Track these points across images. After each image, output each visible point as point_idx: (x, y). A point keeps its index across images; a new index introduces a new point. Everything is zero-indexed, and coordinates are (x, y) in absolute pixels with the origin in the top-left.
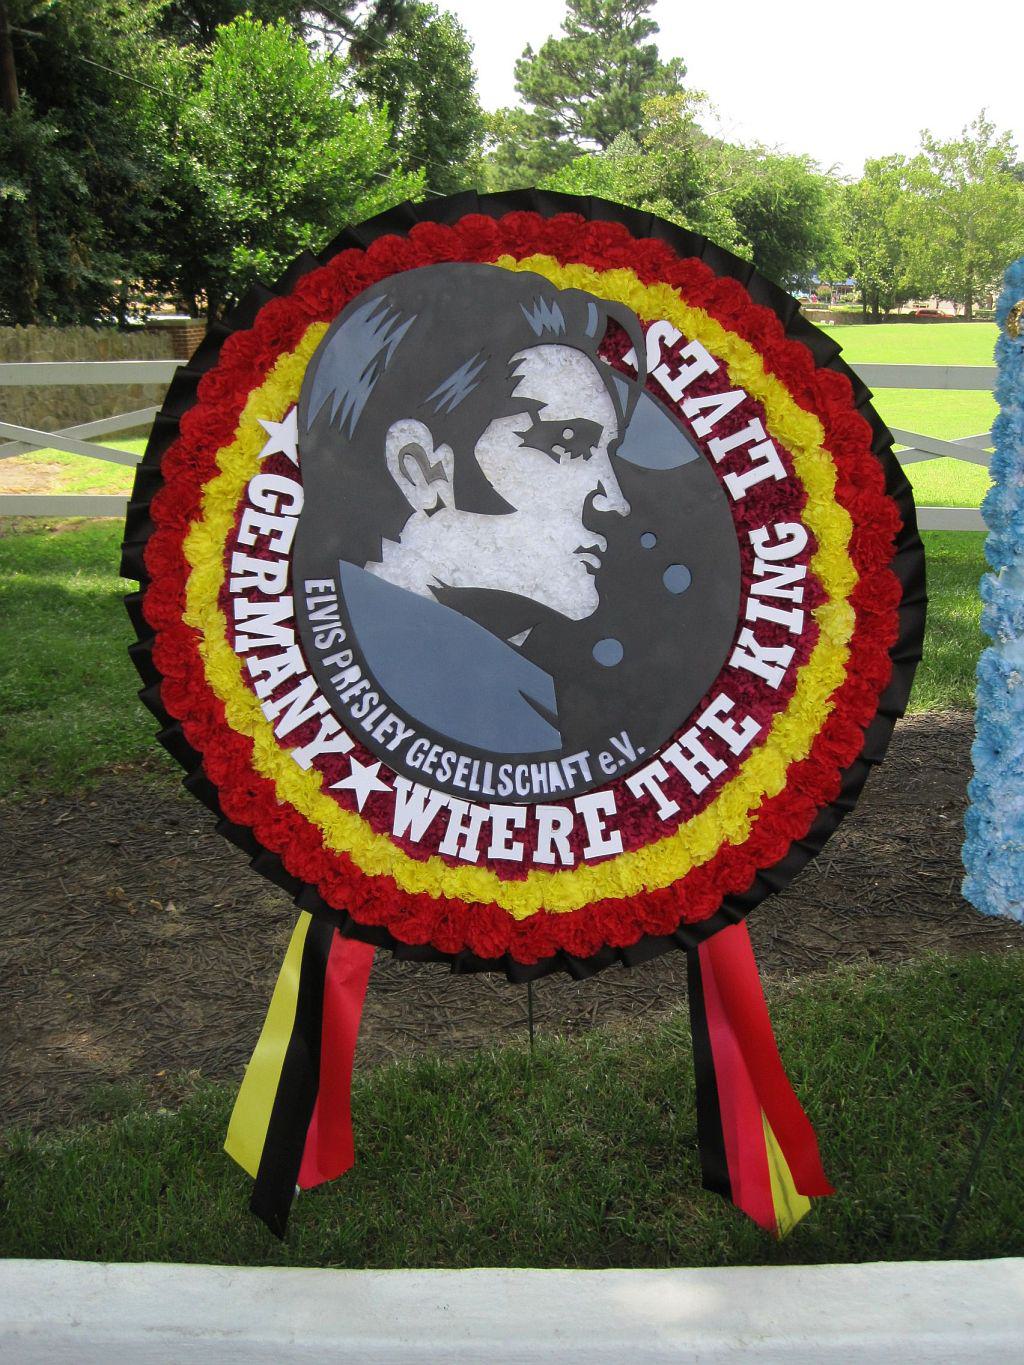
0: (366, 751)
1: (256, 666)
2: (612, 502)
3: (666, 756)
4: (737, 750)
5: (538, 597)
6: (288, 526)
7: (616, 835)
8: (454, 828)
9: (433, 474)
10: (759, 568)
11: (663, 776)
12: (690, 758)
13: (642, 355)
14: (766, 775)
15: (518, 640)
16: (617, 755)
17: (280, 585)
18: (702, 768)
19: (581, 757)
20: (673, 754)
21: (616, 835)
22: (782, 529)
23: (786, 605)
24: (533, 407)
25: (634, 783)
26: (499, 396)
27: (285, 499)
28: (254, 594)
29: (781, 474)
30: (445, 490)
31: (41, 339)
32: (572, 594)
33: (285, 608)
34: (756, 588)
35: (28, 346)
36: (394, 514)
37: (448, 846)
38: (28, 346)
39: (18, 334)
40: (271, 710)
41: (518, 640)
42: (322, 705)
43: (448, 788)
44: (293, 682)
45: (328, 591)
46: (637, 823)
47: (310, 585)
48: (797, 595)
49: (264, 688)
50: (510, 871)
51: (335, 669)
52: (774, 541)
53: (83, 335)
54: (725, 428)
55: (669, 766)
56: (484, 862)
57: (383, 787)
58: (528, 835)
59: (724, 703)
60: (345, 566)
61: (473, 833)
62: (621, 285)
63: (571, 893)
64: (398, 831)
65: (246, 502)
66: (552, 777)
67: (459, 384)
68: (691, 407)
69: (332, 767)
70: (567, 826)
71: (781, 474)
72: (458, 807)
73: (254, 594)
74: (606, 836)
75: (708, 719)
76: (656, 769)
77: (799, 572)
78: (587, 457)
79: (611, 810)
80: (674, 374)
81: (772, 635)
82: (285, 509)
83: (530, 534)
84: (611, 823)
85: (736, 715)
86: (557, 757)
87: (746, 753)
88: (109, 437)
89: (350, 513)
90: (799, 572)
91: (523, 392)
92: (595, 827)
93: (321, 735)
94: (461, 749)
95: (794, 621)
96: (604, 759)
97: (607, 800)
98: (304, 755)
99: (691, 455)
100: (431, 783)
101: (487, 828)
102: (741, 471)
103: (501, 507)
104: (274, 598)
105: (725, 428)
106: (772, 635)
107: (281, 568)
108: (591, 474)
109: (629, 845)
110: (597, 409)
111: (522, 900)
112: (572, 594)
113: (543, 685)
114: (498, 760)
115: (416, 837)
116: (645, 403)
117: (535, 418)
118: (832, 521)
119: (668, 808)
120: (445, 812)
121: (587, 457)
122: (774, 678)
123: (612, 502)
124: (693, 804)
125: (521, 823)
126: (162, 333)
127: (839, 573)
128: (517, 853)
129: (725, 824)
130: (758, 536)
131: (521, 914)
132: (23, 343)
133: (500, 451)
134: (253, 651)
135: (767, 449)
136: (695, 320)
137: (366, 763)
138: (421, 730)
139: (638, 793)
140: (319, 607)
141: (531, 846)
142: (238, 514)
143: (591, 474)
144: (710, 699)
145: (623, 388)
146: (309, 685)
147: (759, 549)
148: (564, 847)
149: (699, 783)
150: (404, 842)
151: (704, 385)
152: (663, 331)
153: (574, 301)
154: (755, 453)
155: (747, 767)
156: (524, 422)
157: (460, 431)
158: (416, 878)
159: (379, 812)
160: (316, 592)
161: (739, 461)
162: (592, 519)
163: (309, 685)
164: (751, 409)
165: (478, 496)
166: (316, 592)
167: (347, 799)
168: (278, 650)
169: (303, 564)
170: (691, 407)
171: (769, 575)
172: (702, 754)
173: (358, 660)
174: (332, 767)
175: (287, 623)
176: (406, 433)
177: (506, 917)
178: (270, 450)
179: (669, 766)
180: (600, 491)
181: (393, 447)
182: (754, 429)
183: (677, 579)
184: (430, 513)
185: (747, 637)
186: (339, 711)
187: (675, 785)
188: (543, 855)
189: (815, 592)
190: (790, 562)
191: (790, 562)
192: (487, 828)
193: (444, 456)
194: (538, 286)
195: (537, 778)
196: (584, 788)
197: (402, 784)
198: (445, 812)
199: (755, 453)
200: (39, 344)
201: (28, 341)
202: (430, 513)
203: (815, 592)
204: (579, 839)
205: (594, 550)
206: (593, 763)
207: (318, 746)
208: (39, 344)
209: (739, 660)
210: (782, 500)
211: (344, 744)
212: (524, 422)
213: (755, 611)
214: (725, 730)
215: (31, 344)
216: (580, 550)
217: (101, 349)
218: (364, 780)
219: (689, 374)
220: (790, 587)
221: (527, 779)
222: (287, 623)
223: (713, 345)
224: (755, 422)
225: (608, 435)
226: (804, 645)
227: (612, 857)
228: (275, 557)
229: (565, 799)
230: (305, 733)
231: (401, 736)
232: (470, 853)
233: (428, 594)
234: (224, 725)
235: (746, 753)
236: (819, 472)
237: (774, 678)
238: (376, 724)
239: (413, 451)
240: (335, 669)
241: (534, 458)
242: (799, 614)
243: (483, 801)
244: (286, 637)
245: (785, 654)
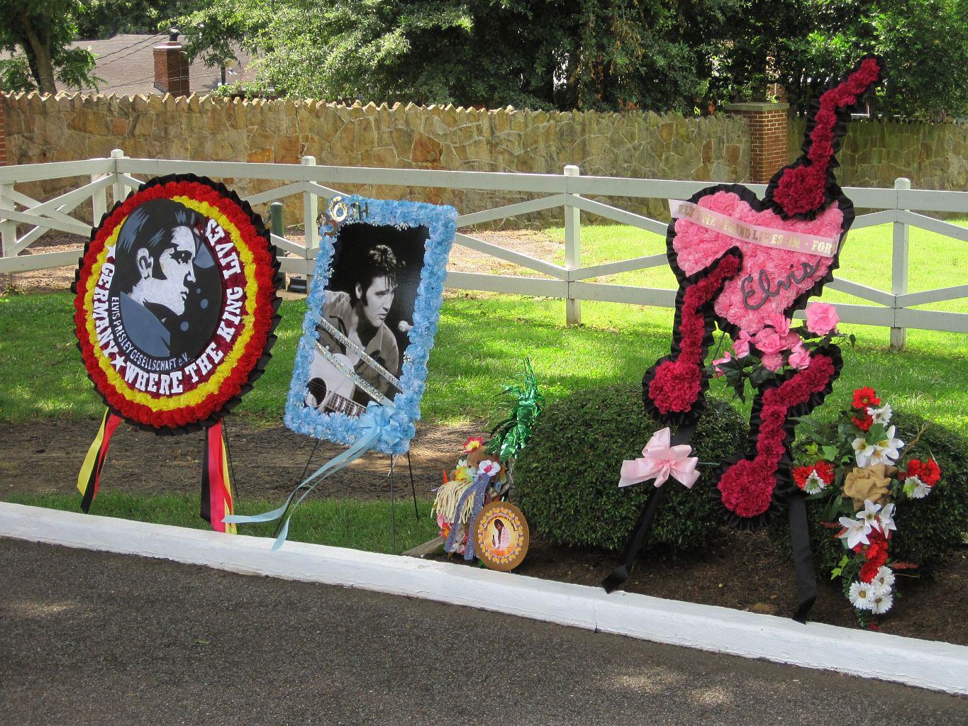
0: (121, 353)
1: (98, 323)
2: (192, 278)
3: (197, 362)
4: (216, 362)
5: (171, 307)
6: (110, 279)
7: (181, 386)
8: (139, 379)
9: (148, 266)
10: (228, 302)
11: (195, 368)
12: (203, 363)
13: (205, 231)
14: (224, 371)
15: (163, 320)
16: (183, 360)
17: (106, 298)
18: (206, 367)
19: (174, 360)
20: (199, 361)
21: (181, 386)
22: (236, 289)
23: (235, 315)
24: (175, 246)
25: (187, 370)
26: (167, 242)
27: (111, 271)
28: (99, 300)
29: (239, 271)
30: (150, 270)
31: (598, 123)
32: (179, 308)
33: (106, 306)
34: (227, 308)
35: (583, 130)
36: (137, 277)
37: (137, 385)
38: (583, 130)
39: (573, 119)
40: (99, 337)
41: (163, 320)
42: (112, 336)
43: (139, 366)
44: (105, 329)
45: (117, 301)
46: (187, 384)
47: (113, 298)
48: (238, 311)
49: (98, 330)
50: (156, 395)
51: (116, 326)
52: (233, 293)
53: (645, 120)
54: (226, 255)
55: (197, 365)
56: (146, 391)
57: (124, 365)
58: (158, 384)
59: (213, 345)
60: (122, 293)
61: (144, 381)
62: (203, 208)
63: (171, 405)
64: (126, 380)
65: (101, 272)
66: (165, 365)
67: (157, 237)
68: (218, 248)
69: (112, 356)
70: (168, 382)
71: (239, 271)
72: (141, 372)
73: (99, 300)
74: (178, 387)
75: (208, 350)
76: (193, 366)
77: (240, 304)
78: (187, 263)
79: (180, 378)
80: (213, 237)
81: (229, 324)
82: (111, 275)
83: (167, 288)
84: (180, 382)
85: (216, 350)
86: (167, 359)
87: (222, 361)
88: (483, 227)
89: (126, 278)
90: (240, 304)
91: (173, 241)
92: (175, 383)
93: (110, 347)
94: (145, 354)
95: (236, 320)
96: (180, 361)
97: (179, 374)
98: (106, 352)
99: (211, 263)
100: (135, 364)
101: (148, 380)
102: (228, 270)
103: (163, 277)
104: (104, 302)
105: (226, 255)
106: (229, 324)
107: (107, 293)
108: (189, 268)
109: (185, 391)
110: (193, 250)
111: (155, 405)
112: (179, 308)
113: (167, 335)
114: (154, 358)
115: (130, 382)
116: (203, 245)
117: (175, 249)
118: (252, 287)
119: (195, 379)
120: (138, 374)
121: (187, 263)
122: (228, 339)
123: (192, 278)
124: (204, 379)
125: (156, 380)
126: (737, 117)
127: (251, 305)
128: (154, 389)
129: (212, 386)
130: (229, 291)
131: (154, 410)
132: (578, 128)
133: (166, 259)
134: (97, 319)
135: (236, 263)
136: (223, 219)
137: (121, 356)
138: (136, 348)
139: (188, 373)
140: (115, 306)
141: (158, 389)
142: (100, 275)
143: (189, 268)
144: (207, 345)
145: (198, 241)
146: (110, 330)
147: (229, 296)
148: (167, 388)
149: (204, 372)
150: (127, 383)
151: (220, 241)
152: (212, 223)
153: (189, 212)
154: (232, 264)
155: (218, 368)
156: (172, 251)
157: (156, 253)
158: (128, 395)
159: (123, 371)
160: (114, 301)
161: (229, 266)
162: (186, 283)
163: (110, 330)
164: (234, 249)
165: (158, 274)
166: (114, 301)
167: (114, 366)
168: (102, 319)
169: (113, 292)
170: (218, 248)
171: (232, 304)
172: (207, 362)
173: (122, 324)
174: (112, 356)
175: (106, 310)
176: (143, 252)
177: (149, 409)
178: (109, 256)
179: (197, 365)
180: (189, 274)
181: (139, 257)
182: (234, 255)
183: (204, 304)
184: (145, 278)
185: (222, 324)
186: (115, 339)
187: (198, 371)
188: (161, 391)
189: (244, 312)
190: (237, 300)
191: (237, 300)
192: (148, 380)
193: (151, 260)
194: (181, 206)
195: (162, 365)
196: (173, 370)
197: (128, 363)
198: (138, 374)
199: (232, 264)
200: (595, 127)
201: (583, 125)
202: (145, 278)
203: (244, 312)
204: (171, 386)
205: (185, 293)
206: (177, 361)
207: (109, 350)
208: (595, 127)
209: (219, 332)
210: (239, 280)
211: (116, 350)
212: (172, 251)
213: (226, 316)
214: (213, 354)
215: (587, 128)
216: (182, 293)
217: (664, 134)
218: (119, 361)
219: (217, 237)
220: (236, 309)
221: (159, 366)
222: (106, 310)
223: (225, 228)
224: (234, 254)
225: (194, 255)
226: (240, 328)
227: (180, 394)
228: (106, 289)
229: (167, 373)
230: (106, 346)
231: (130, 349)
232: (143, 388)
233: (142, 304)
234: (88, 341)
235: (222, 361)
236: (250, 270)
237: (228, 339)
238: (124, 344)
239: (144, 258)
240: (116, 326)
241: (174, 261)
242: (239, 318)
243: (148, 372)
244: (105, 315)
245: (232, 331)
